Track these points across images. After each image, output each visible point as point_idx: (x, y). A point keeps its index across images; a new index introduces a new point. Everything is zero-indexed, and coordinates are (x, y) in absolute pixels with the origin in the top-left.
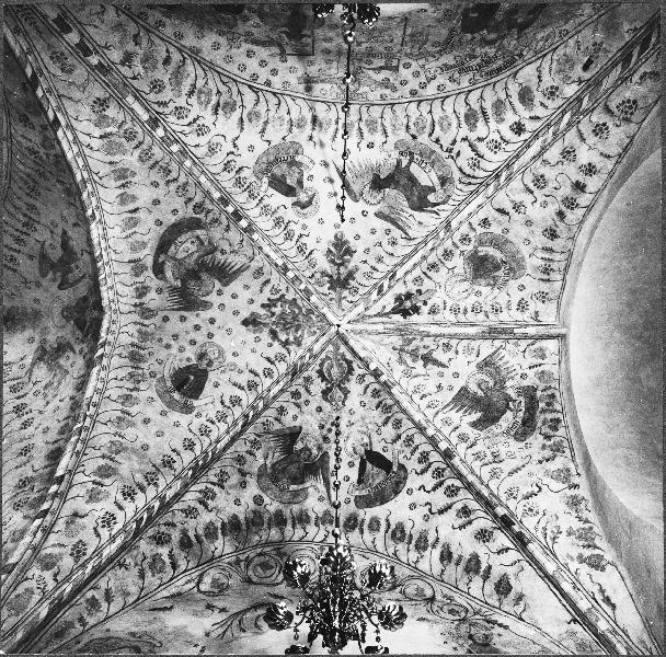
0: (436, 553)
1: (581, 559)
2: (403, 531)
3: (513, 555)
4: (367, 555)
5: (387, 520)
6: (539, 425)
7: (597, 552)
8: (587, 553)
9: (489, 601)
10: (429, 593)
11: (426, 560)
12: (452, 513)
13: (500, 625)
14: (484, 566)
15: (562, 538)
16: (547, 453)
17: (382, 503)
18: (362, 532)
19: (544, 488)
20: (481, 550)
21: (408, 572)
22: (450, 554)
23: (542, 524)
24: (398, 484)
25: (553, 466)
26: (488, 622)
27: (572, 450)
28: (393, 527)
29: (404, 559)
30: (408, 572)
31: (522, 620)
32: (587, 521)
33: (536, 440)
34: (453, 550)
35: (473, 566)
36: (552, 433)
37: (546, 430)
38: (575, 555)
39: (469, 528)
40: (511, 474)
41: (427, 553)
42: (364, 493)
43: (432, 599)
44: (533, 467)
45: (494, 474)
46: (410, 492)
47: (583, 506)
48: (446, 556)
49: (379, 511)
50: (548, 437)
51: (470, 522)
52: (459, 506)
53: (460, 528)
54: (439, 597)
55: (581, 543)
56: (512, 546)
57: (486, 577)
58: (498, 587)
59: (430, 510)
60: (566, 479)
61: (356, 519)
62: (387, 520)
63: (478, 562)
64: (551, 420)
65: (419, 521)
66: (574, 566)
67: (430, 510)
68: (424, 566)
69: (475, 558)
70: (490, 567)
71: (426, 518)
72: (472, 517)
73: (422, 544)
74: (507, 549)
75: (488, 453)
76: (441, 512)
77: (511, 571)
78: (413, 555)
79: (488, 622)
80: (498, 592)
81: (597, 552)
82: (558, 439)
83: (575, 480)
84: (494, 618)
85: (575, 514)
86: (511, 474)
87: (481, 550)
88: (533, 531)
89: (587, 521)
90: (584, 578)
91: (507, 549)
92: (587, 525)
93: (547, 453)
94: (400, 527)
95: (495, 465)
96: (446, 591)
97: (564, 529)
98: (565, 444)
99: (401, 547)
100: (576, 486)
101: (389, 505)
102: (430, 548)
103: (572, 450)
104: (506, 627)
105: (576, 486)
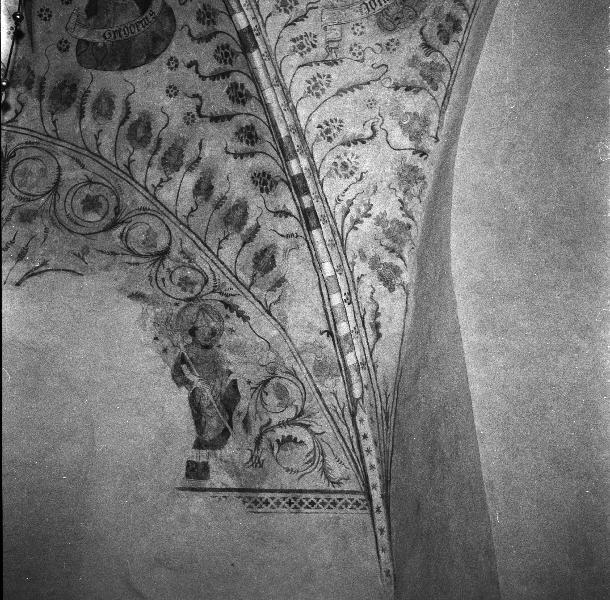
0: (190, 181)
1: (375, 263)
2: (148, 128)
3: (292, 225)
4: (86, 161)
5: (127, 103)
6: (427, 13)
7: (399, 263)
8: (387, 258)
9: (240, 274)
10: (162, 242)
11: (173, 186)
12: (230, 128)
13: (240, 314)
14: (251, 223)
15: (367, 225)
16: (414, 75)
17: (123, 68)
18: (81, 115)
19: (381, 136)
20: (256, 203)
21: (141, 201)
22: (211, 188)
23: (349, 196)
24: (156, 39)
25: (413, 104)
26: (227, 305)
27: (447, 96)
28: (135, 117)
29: (140, 177)
30: (141, 201)
31: (269, 313)
32: (408, 215)
33: (409, 42)
34: (216, 183)
35: (235, 217)
36: (436, 42)
37: (431, 30)
38: (370, 253)
39: (249, 163)
40: (341, 92)
41: (177, 176)
42: (96, 38)
43: (164, 254)
44: (384, 94)
45: (314, 88)
46: (173, 63)
47: (415, 189)
48: (204, 189)
49: (112, 80)
50: (427, 47)
51: (252, 154)
52: (245, 121)
53: (236, 155)
54: (175, 253)
55: (386, 242)
56: (294, 212)
57: (248, 240)
58: (259, 257)
59: (199, 109)
60: (415, 137)
61: (74, 88)
62: (127, 103)
63: (245, 215)
64: (449, 17)
65: (177, 121)
66: (362, 268)
67: (199, 109)
68: (167, 195)
69: (242, 207)
70: (257, 228)
71: (189, 119)
72: (257, 147)
73: (172, 160)
74: (287, 214)
75: (321, 40)
76: (215, 119)
77: (282, 243)
78: (155, 175)
79: (227, 305)
80: (256, 265)
81: (399, 263)
82: (440, 60)
83: (428, 144)
84: (236, 301)
85: (400, 195)
86: (341, 92)
87: (256, 203)
88: (332, 203)
89: (408, 215)
90: (365, 291)
91: (287, 214)
92: (406, 220)
93: (414, 75)
94: (145, 121)
95: (322, 69)
96: (187, 245)
97: (376, 211)
98: (446, 76)
99: (139, 156)
100: (423, 153)
101: (137, 76)
102: (183, 170)
103: (447, 96)
104: (246, 319)
105: (423, 153)
